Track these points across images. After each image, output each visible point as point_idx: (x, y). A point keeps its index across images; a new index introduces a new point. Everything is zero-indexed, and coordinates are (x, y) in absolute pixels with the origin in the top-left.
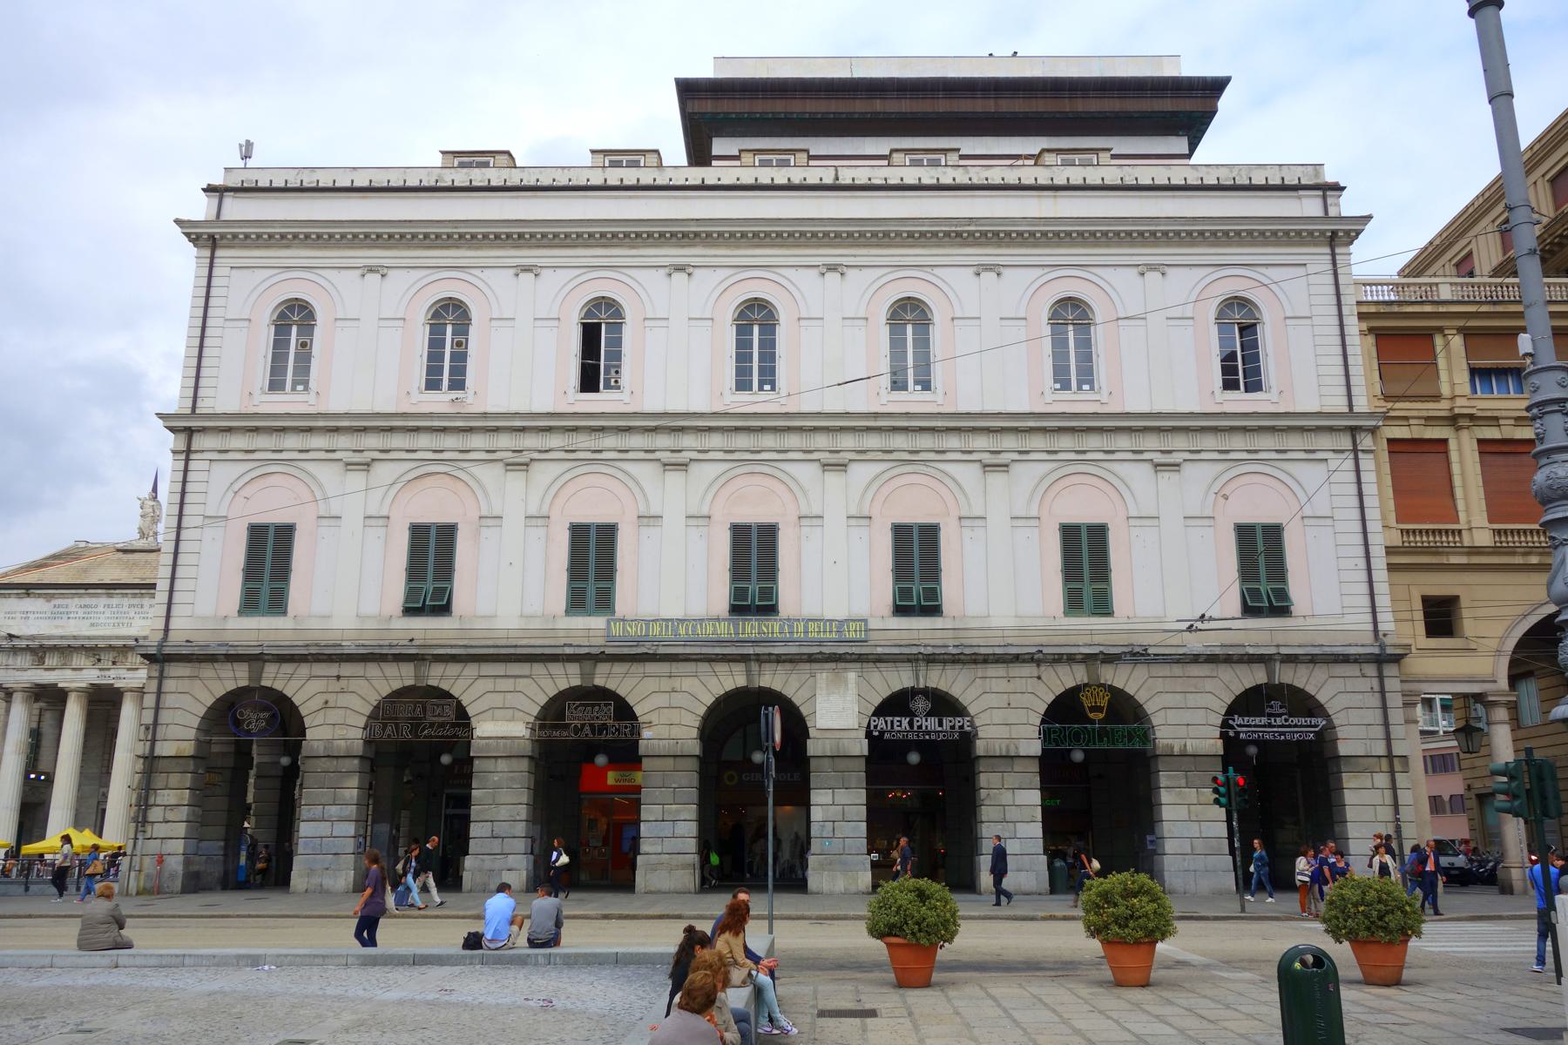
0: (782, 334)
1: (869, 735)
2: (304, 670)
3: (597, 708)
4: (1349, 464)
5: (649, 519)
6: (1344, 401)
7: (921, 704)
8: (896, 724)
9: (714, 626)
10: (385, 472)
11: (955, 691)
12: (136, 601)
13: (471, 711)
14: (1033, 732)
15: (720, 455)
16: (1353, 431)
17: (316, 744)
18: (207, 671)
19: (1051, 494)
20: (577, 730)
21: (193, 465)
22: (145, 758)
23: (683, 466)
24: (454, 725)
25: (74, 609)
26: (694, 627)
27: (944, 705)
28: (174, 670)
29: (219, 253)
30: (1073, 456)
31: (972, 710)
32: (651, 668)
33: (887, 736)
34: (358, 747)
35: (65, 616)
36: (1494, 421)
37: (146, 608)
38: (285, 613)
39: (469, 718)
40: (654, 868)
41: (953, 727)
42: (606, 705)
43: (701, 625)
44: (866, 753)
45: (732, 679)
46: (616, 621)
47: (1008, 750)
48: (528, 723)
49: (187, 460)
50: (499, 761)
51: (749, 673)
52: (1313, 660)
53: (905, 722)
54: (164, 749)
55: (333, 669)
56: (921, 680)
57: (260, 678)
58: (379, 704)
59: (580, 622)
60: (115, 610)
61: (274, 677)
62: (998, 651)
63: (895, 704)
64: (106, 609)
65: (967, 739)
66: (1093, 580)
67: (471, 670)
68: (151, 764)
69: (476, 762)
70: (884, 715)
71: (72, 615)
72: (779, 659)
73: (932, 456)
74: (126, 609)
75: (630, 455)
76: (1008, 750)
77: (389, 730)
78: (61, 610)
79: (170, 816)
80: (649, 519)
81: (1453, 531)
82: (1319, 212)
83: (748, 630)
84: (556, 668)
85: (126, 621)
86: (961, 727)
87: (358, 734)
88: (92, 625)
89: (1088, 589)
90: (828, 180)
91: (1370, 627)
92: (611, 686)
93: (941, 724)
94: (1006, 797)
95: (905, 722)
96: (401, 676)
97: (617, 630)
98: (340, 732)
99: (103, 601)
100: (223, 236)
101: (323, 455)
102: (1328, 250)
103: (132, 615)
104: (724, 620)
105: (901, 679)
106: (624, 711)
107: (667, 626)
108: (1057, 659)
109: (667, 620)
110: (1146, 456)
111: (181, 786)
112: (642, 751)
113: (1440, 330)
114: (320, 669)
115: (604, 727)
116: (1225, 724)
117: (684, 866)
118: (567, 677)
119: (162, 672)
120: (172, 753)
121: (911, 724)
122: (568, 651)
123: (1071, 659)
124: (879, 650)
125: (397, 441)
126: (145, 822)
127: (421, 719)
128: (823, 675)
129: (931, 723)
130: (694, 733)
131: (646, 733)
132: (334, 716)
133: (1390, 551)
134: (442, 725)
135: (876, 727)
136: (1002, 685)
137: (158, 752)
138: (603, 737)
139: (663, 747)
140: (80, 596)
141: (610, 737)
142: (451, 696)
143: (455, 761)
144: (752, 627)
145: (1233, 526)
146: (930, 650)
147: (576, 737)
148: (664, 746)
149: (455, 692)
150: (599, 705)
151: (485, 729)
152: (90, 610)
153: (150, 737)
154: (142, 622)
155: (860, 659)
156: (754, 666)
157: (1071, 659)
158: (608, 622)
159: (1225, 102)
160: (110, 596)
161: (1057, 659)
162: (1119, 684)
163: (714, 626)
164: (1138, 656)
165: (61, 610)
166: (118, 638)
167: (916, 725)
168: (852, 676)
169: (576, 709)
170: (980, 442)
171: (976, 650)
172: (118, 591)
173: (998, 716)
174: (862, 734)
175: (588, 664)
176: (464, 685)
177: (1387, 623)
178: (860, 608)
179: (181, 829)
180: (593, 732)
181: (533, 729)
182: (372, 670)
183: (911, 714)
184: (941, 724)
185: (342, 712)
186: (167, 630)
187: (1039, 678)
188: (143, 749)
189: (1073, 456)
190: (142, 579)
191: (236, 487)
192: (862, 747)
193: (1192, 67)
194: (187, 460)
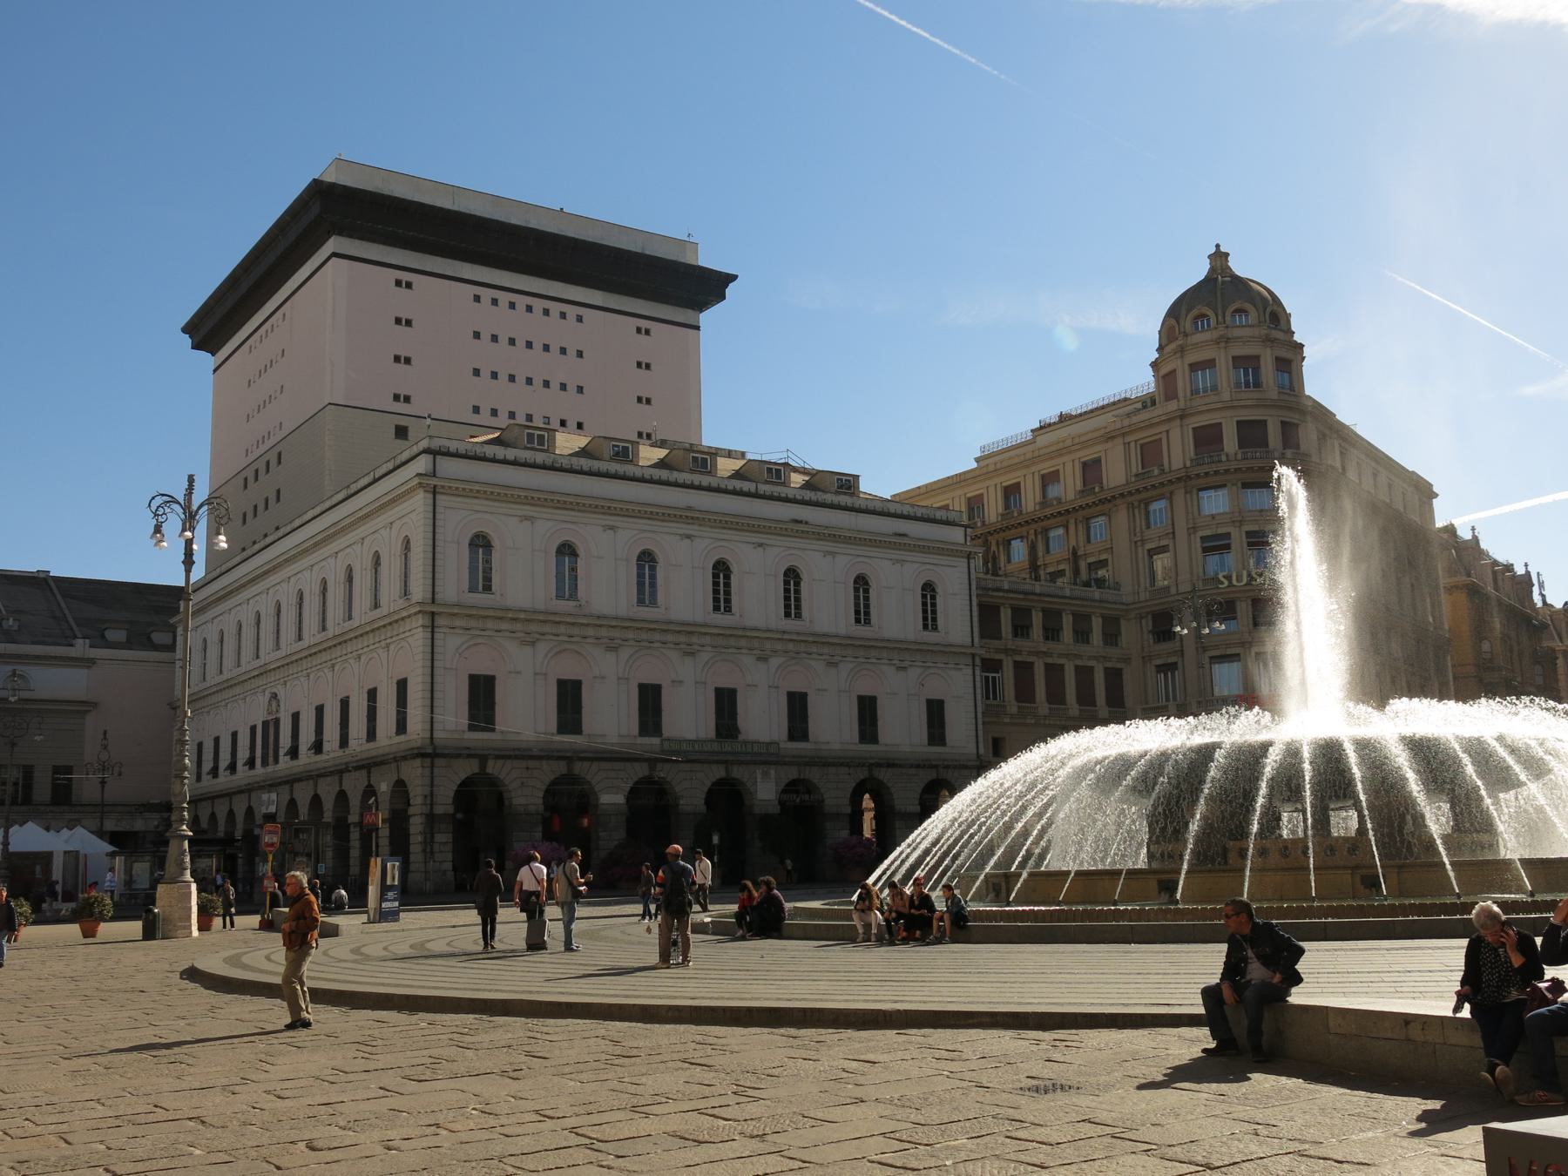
0: (734, 580)
1: (780, 802)
4: (970, 672)
5: (677, 682)
10: (542, 647)
14: (847, 801)
15: (710, 649)
16: (973, 656)
21: (436, 636)
22: (427, 815)
23: (692, 654)
28: (439, 762)
29: (439, 497)
30: (863, 660)
36: (1019, 653)
45: (718, 772)
49: (433, 632)
51: (727, 770)
52: (955, 767)
54: (439, 810)
61: (492, 767)
68: (431, 819)
72: (741, 763)
73: (805, 655)
75: (666, 646)
80: (677, 682)
84: (636, 765)
87: (541, 801)
90: (753, 490)
91: (975, 751)
100: (443, 487)
101: (508, 634)
102: (966, 560)
105: (793, 773)
110: (894, 662)
113: (1003, 604)
116: (920, 799)
118: (641, 770)
119: (432, 763)
124: (787, 759)
125: (547, 628)
126: (432, 853)
130: (703, 802)
131: (681, 802)
144: (728, 746)
153: (428, 802)
155: (776, 763)
158: (662, 741)
159: (731, 290)
162: (881, 777)
164: (891, 764)
170: (826, 650)
177: (982, 751)
178: (775, 738)
179: (450, 857)
186: (432, 738)
188: (426, 810)
189: (863, 660)
191: (460, 651)
193: (709, 259)
194: (433, 632)
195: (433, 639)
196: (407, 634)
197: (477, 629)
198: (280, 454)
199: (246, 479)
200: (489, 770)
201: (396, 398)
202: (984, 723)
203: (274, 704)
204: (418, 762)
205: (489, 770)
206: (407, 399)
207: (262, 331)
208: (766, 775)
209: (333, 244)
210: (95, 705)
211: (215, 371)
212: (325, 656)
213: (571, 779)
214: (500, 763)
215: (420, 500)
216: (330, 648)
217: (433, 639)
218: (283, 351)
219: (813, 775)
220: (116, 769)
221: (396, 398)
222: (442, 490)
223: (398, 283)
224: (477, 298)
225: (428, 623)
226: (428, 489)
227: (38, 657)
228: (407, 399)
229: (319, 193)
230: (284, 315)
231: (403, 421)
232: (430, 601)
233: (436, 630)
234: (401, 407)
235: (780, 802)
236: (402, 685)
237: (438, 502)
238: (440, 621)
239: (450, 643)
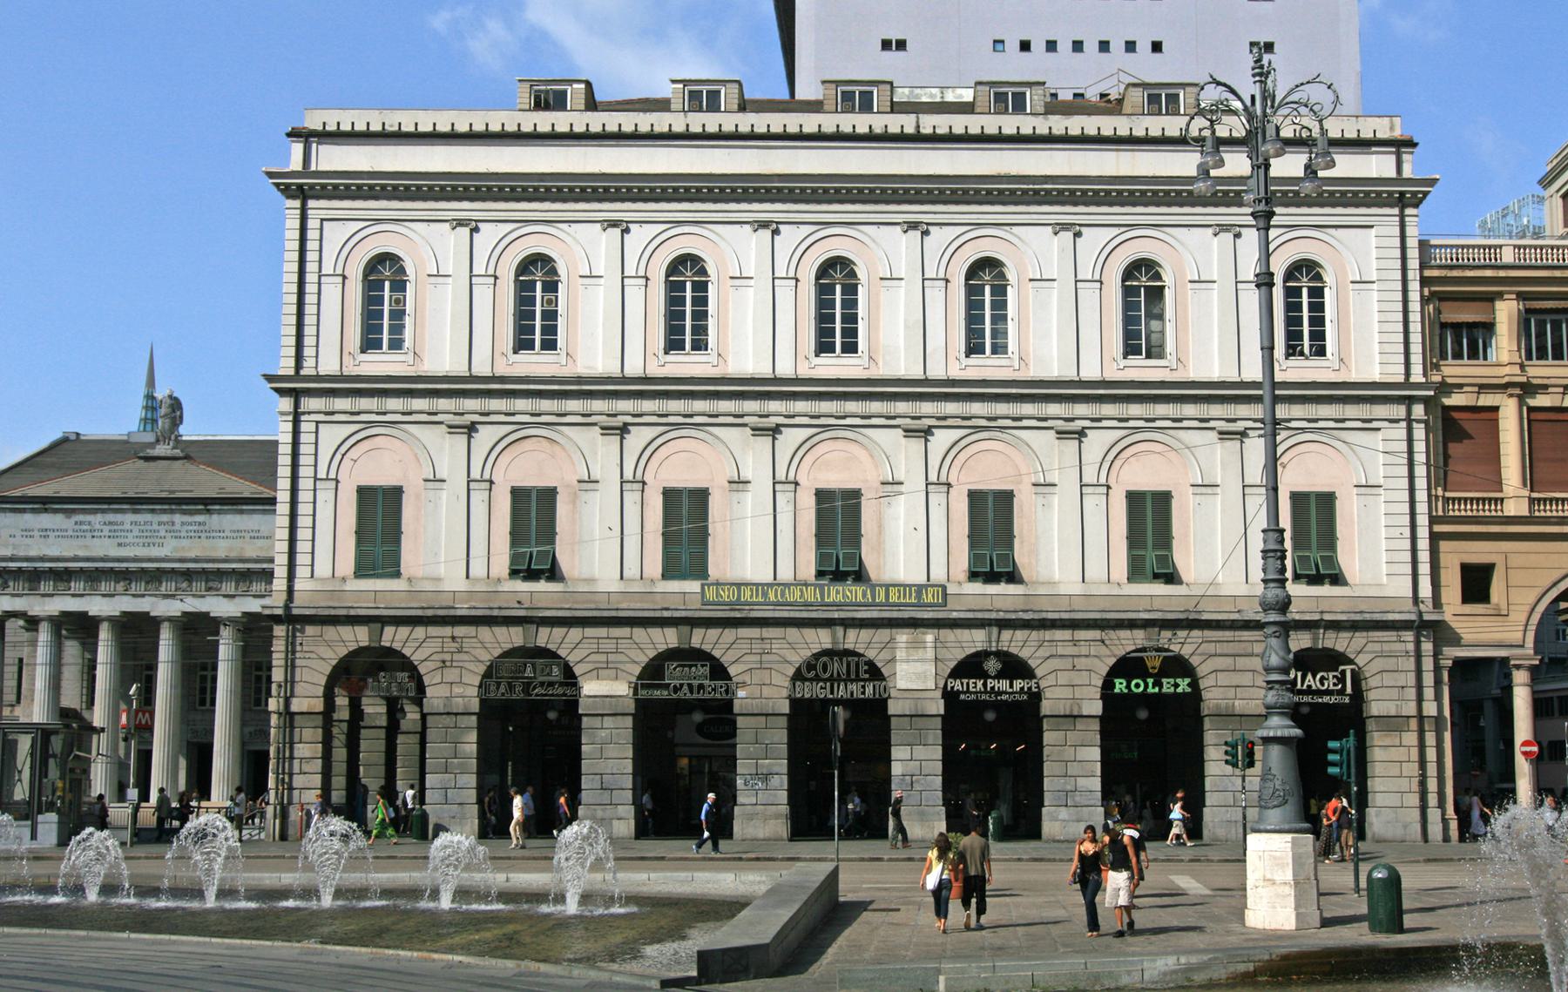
2: (420, 632)
3: (693, 669)
6: (1402, 369)
7: (992, 665)
8: (971, 685)
9: (801, 591)
11: (1024, 654)
12: (165, 518)
13: (577, 670)
14: (1096, 693)
17: (435, 701)
18: (330, 632)
19: (1118, 463)
20: (676, 690)
24: (561, 684)
25: (98, 526)
26: (783, 594)
27: (1015, 667)
31: (1039, 673)
32: (745, 632)
33: (962, 697)
34: (475, 705)
35: (89, 534)
37: (177, 527)
38: (397, 575)
39: (576, 678)
40: (750, 817)
41: (1022, 689)
42: (702, 666)
43: (789, 589)
44: (942, 712)
46: (709, 585)
47: (1072, 710)
48: (630, 683)
50: (606, 718)
51: (834, 636)
53: (980, 684)
55: (447, 631)
56: (994, 644)
58: (492, 664)
59: (675, 586)
60: (142, 528)
61: (392, 637)
62: (1065, 616)
63: (970, 667)
64: (133, 527)
65: (1036, 697)
66: (1155, 547)
67: (575, 633)
69: (585, 719)
70: (960, 678)
71: (95, 534)
74: (155, 527)
76: (1072, 710)
77: (502, 689)
78: (85, 527)
79: (306, 768)
81: (1496, 500)
82: (1392, 174)
83: (833, 593)
85: (158, 541)
86: (1030, 688)
87: (474, 691)
88: (120, 545)
89: (1151, 555)
92: (707, 647)
93: (1011, 686)
94: (1069, 753)
95: (980, 684)
96: (513, 637)
97: (711, 594)
98: (457, 690)
99: (129, 518)
103: (162, 533)
104: (811, 585)
105: (976, 640)
106: (719, 671)
107: (757, 590)
108: (1119, 624)
109: (757, 585)
111: (314, 740)
112: (736, 709)
114: (434, 631)
115: (701, 687)
117: (777, 816)
120: (305, 709)
121: (985, 685)
122: (666, 614)
123: (1132, 624)
124: (955, 615)
127: (531, 678)
128: (903, 636)
129: (1003, 685)
131: (741, 693)
132: (451, 675)
133: (1433, 520)
134: (551, 684)
135: (952, 688)
136: (1070, 650)
137: (294, 708)
138: (700, 696)
139: (755, 706)
140: (103, 511)
141: (707, 696)
142: (561, 658)
143: (561, 713)
144: (837, 593)
145: (1288, 495)
146: (1001, 615)
147: (675, 696)
148: (757, 706)
149: (562, 653)
150: (696, 666)
151: (590, 688)
152: (116, 527)
154: (174, 543)
156: (840, 630)
157: (1132, 624)
158: (703, 586)
160: (136, 511)
161: (1119, 624)
163: (801, 591)
165: (85, 527)
166: (150, 560)
167: (989, 686)
168: (929, 637)
169: (675, 669)
171: (1044, 615)
172: (144, 507)
173: (1063, 678)
174: (939, 694)
175: (685, 629)
176: (568, 643)
178: (938, 574)
180: (692, 692)
181: (636, 689)
182: (485, 632)
183: (984, 676)
184: (1011, 686)
185: (457, 671)
187: (1103, 641)
192: (939, 707)
202: (1435, 538)
208: (917, 645)
214: (404, 631)
219: (1016, 643)
235: (949, 696)
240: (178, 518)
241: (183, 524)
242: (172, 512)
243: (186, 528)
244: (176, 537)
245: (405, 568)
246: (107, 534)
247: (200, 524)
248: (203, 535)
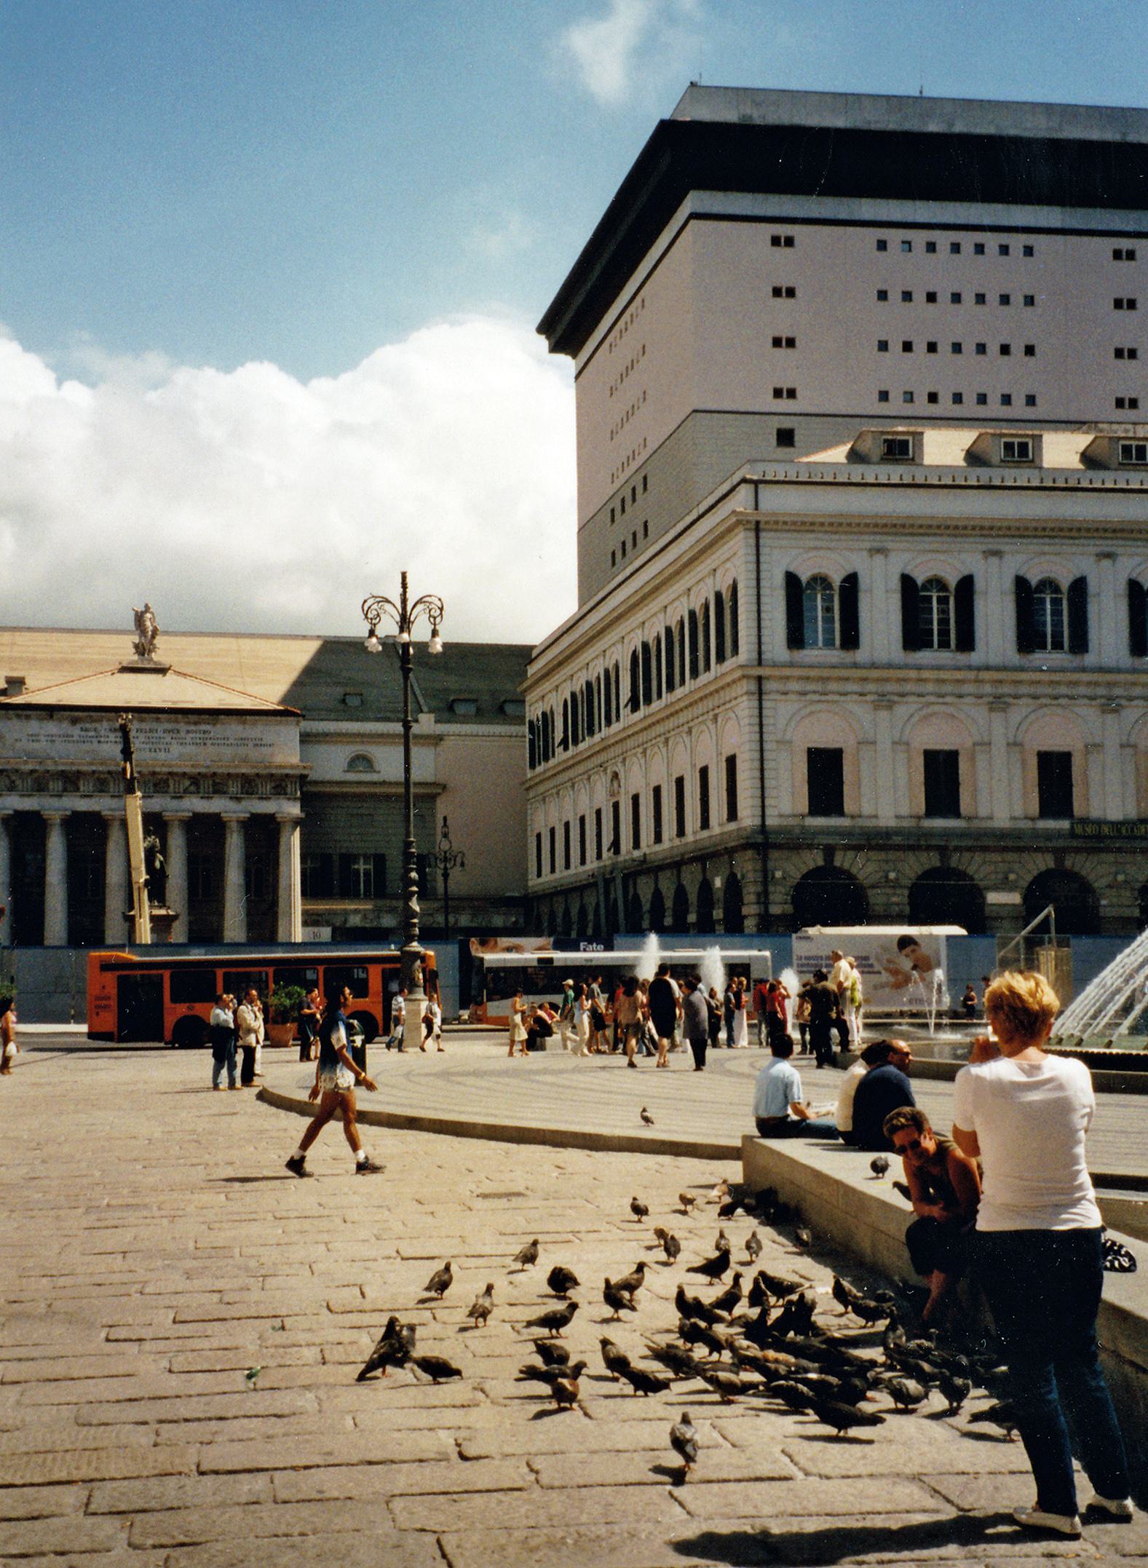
10: (902, 710)
17: (877, 908)
21: (765, 704)
22: (759, 915)
26: (1132, 829)
29: (763, 534)
37: (183, 734)
38: (840, 812)
54: (775, 910)
57: (832, 861)
61: (841, 860)
64: (138, 734)
100: (767, 523)
103: (168, 739)
190: (173, 702)
195: (761, 708)
196: (734, 703)
197: (814, 692)
198: (645, 478)
199: (613, 511)
200: (837, 863)
201: (778, 393)
203: (615, 784)
204: (750, 853)
205: (837, 863)
206: (792, 394)
207: (621, 324)
209: (693, 201)
210: (444, 787)
211: (577, 377)
212: (659, 729)
213: (943, 872)
215: (740, 543)
216: (663, 719)
217: (761, 708)
218: (644, 347)
220: (459, 860)
221: (778, 393)
222: (767, 527)
223: (776, 241)
224: (882, 245)
225: (753, 686)
226: (748, 526)
227: (381, 735)
228: (792, 394)
229: (668, 133)
230: (643, 301)
231: (787, 423)
232: (756, 663)
233: (764, 697)
234: (784, 405)
236: (731, 762)
237: (761, 541)
238: (768, 686)
239: (781, 711)
240: (183, 727)
241: (188, 732)
242: (177, 721)
243: (191, 735)
244: (181, 744)
245: (848, 806)
246: (113, 740)
247: (205, 732)
248: (209, 742)
